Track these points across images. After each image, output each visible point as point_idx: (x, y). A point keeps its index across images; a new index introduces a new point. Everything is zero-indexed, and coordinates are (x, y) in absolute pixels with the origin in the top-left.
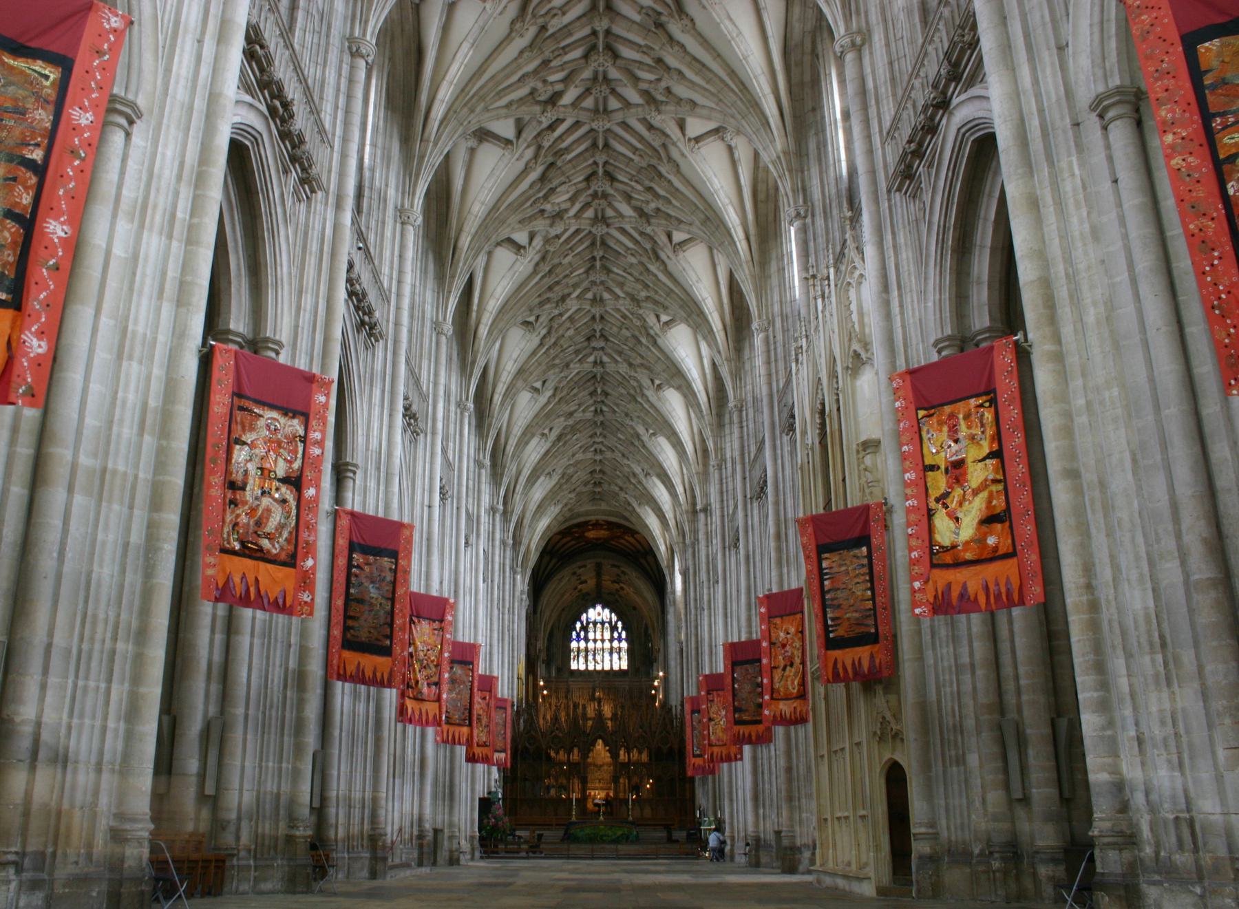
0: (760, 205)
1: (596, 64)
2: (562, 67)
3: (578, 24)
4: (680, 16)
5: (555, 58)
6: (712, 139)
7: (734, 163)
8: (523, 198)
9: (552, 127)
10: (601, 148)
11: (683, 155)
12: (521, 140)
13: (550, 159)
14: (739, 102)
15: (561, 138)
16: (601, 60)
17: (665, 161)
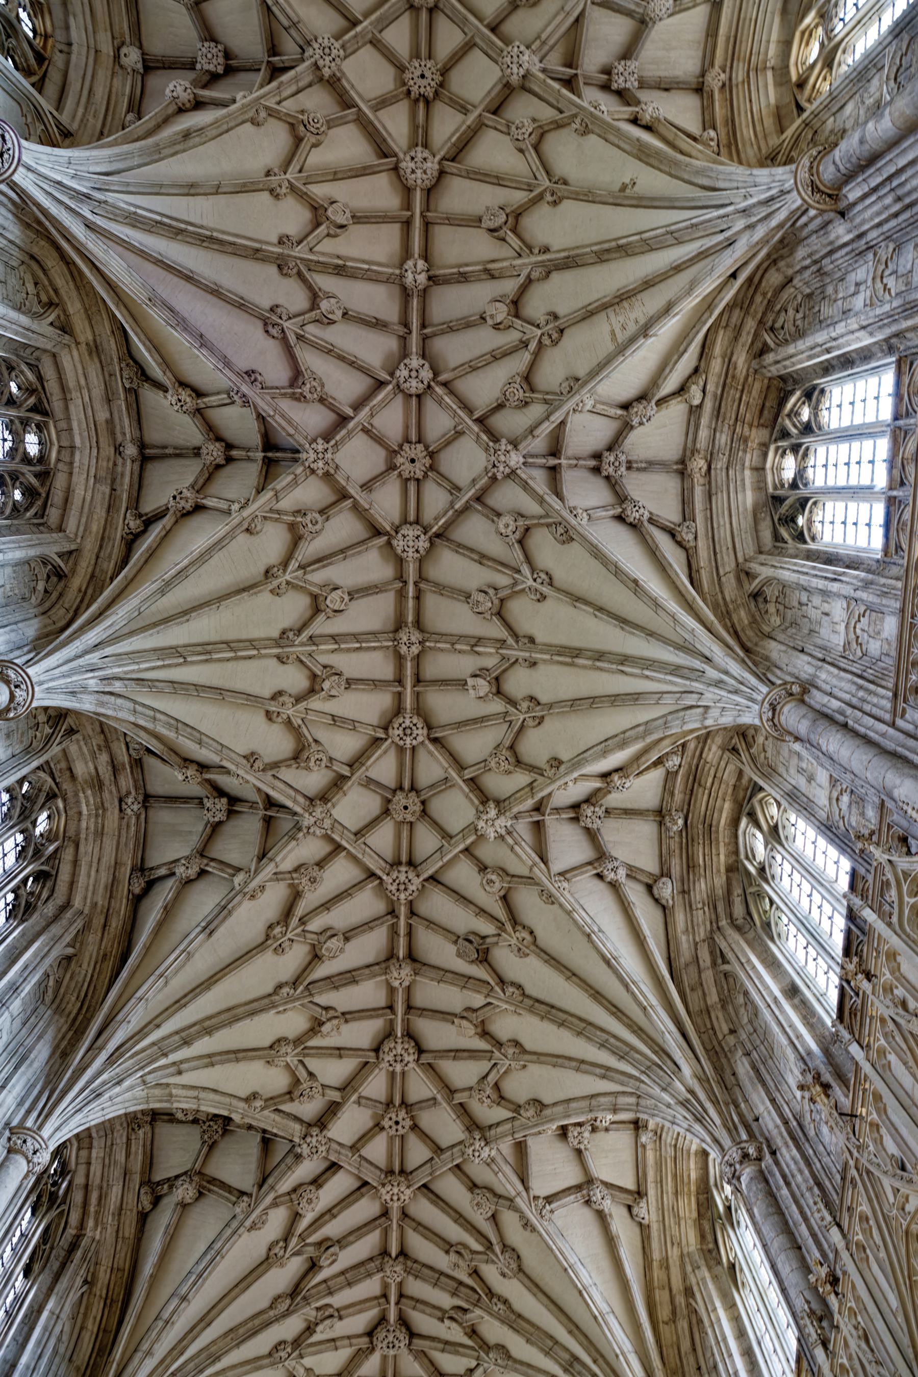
0: (665, 1331)
1: (389, 1058)
2: (340, 1052)
3: (367, 971)
4: (514, 928)
5: (329, 1020)
6: (572, 1197)
7: (611, 1242)
8: (257, 1322)
9: (317, 1182)
10: (394, 1255)
11: (527, 1225)
12: (265, 1187)
13: (310, 1251)
14: (612, 1040)
15: (330, 1213)
16: (399, 1050)
17: (497, 1249)
